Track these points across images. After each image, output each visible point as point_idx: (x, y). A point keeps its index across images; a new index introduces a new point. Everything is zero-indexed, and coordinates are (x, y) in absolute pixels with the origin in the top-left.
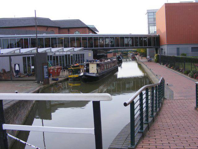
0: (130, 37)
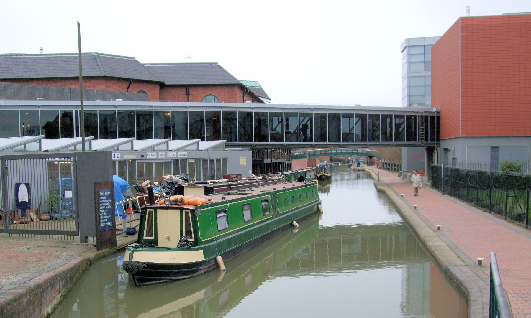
0: (357, 116)
